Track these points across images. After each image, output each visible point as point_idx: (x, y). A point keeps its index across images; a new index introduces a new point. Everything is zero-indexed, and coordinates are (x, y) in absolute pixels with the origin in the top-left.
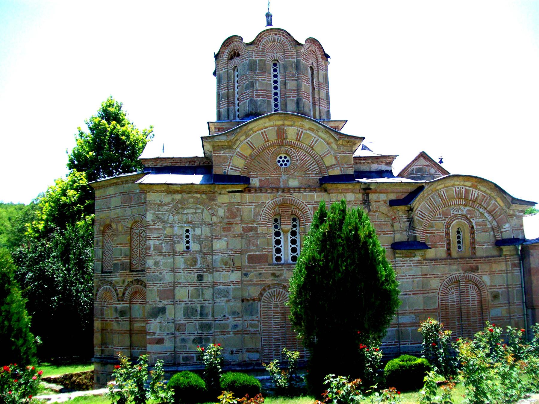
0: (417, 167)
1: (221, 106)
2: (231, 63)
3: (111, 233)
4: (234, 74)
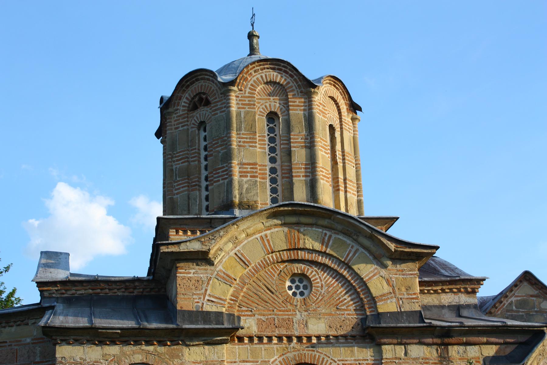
0: (519, 298)
1: (176, 190)
2: (193, 117)
4: (199, 134)
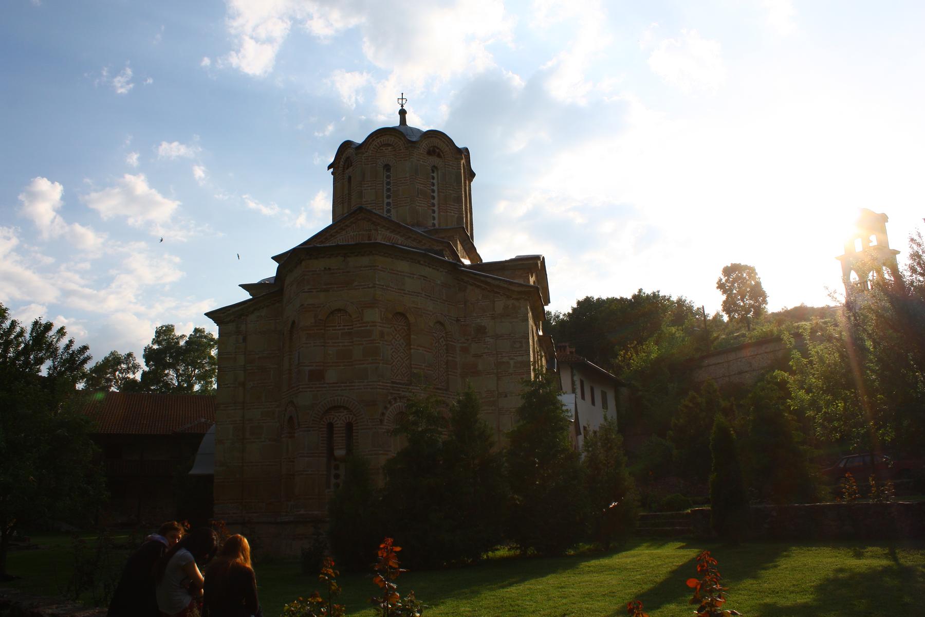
1: (418, 203)
3: (400, 327)
